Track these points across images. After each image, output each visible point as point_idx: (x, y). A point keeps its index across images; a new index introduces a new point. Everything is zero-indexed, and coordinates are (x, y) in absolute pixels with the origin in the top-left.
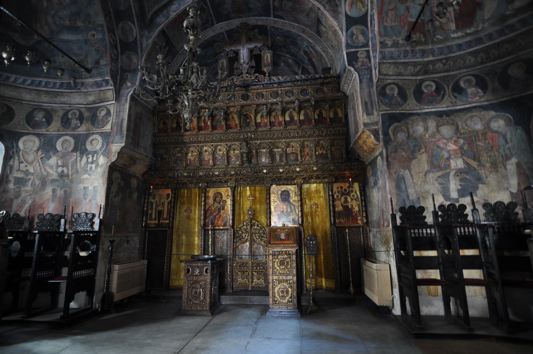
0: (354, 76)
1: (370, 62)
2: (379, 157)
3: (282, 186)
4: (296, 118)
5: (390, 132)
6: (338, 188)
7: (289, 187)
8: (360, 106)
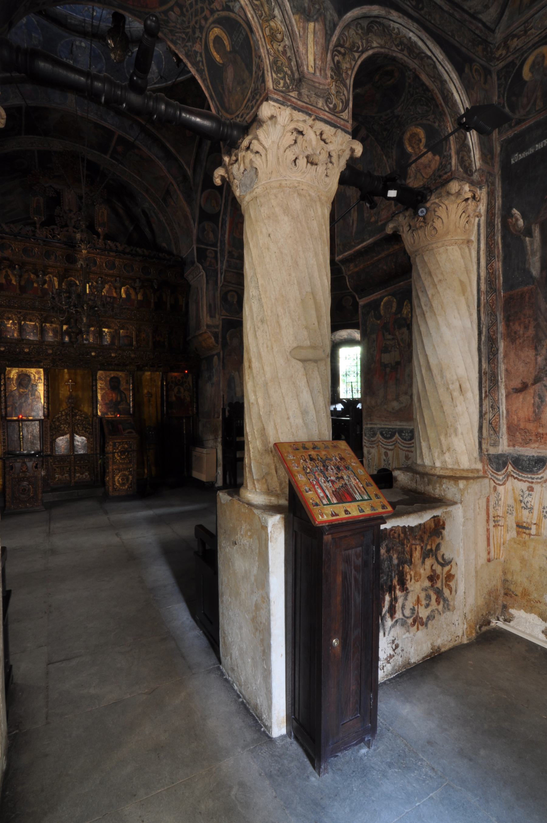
0: (202, 273)
1: (217, 265)
2: (216, 357)
3: (112, 372)
4: (133, 297)
5: (227, 336)
6: (172, 378)
7: (120, 374)
8: (205, 307)
